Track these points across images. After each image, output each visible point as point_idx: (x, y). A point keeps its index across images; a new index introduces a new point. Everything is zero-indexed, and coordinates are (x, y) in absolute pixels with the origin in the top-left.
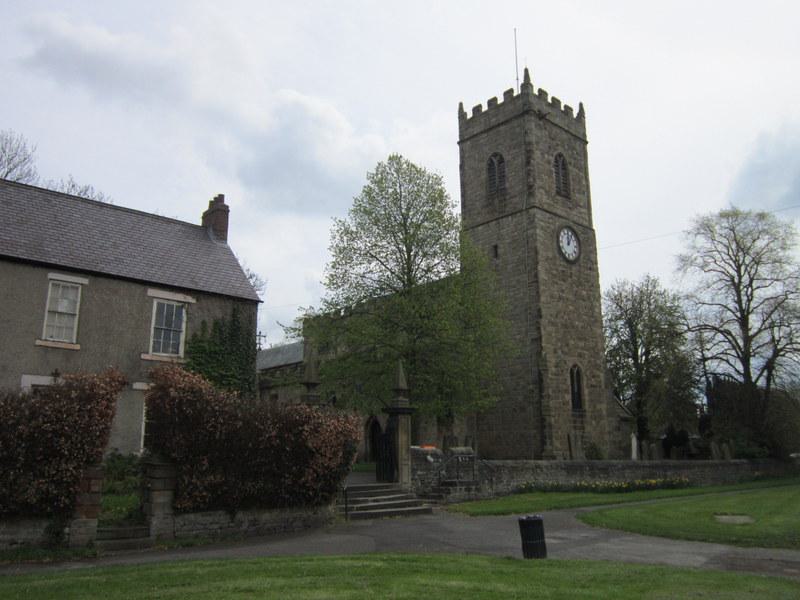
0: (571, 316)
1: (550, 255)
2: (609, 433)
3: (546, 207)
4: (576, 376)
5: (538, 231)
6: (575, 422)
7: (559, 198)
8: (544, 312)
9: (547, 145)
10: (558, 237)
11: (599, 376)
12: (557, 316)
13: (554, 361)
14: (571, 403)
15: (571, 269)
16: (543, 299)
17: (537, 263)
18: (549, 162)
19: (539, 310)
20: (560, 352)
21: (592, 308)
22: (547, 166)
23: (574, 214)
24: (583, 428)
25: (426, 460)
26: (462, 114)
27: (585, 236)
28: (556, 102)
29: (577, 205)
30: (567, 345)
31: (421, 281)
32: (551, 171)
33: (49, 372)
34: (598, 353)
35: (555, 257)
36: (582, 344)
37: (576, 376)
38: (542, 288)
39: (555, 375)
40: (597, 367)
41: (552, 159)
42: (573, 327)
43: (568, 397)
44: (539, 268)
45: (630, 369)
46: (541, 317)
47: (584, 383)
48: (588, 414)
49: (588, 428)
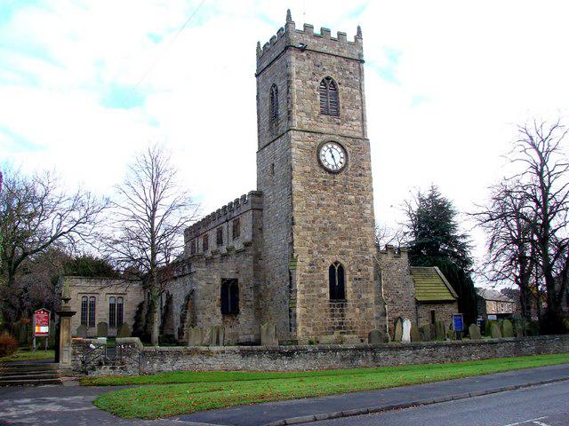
0: (332, 220)
1: (308, 169)
2: (377, 318)
3: (306, 128)
4: (337, 273)
5: (293, 150)
6: (332, 311)
7: (323, 117)
8: (297, 219)
9: (311, 72)
10: (318, 152)
11: (367, 270)
12: (313, 222)
13: (308, 260)
14: (328, 295)
15: (334, 178)
16: (295, 209)
17: (292, 178)
18: (313, 87)
19: (293, 219)
20: (316, 253)
21: (362, 209)
22: (311, 91)
23: (344, 129)
24: (343, 316)
25: (89, 347)
26: (258, 47)
27: (357, 148)
28: (325, 32)
29: (348, 119)
30: (326, 246)
31: (337, 160)
32: (315, 95)
33: (263, 188)
34: (366, 250)
35: (314, 170)
36: (346, 243)
37: (337, 273)
38: (295, 198)
39: (310, 272)
40: (364, 261)
41: (317, 84)
42: (335, 229)
43: (326, 290)
44: (294, 182)
45: (17, 319)
46: (293, 224)
47: (347, 277)
48: (350, 304)
49: (349, 316)
